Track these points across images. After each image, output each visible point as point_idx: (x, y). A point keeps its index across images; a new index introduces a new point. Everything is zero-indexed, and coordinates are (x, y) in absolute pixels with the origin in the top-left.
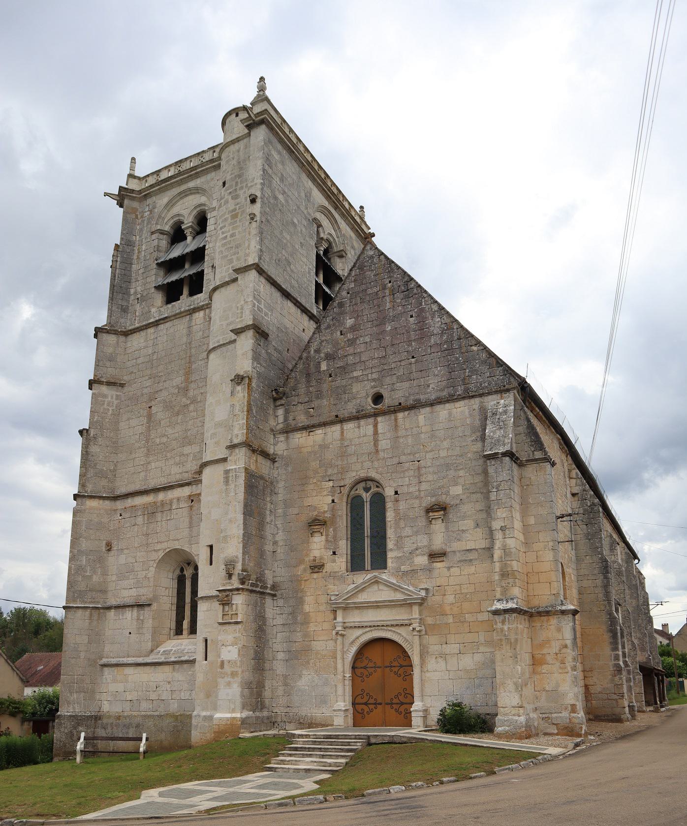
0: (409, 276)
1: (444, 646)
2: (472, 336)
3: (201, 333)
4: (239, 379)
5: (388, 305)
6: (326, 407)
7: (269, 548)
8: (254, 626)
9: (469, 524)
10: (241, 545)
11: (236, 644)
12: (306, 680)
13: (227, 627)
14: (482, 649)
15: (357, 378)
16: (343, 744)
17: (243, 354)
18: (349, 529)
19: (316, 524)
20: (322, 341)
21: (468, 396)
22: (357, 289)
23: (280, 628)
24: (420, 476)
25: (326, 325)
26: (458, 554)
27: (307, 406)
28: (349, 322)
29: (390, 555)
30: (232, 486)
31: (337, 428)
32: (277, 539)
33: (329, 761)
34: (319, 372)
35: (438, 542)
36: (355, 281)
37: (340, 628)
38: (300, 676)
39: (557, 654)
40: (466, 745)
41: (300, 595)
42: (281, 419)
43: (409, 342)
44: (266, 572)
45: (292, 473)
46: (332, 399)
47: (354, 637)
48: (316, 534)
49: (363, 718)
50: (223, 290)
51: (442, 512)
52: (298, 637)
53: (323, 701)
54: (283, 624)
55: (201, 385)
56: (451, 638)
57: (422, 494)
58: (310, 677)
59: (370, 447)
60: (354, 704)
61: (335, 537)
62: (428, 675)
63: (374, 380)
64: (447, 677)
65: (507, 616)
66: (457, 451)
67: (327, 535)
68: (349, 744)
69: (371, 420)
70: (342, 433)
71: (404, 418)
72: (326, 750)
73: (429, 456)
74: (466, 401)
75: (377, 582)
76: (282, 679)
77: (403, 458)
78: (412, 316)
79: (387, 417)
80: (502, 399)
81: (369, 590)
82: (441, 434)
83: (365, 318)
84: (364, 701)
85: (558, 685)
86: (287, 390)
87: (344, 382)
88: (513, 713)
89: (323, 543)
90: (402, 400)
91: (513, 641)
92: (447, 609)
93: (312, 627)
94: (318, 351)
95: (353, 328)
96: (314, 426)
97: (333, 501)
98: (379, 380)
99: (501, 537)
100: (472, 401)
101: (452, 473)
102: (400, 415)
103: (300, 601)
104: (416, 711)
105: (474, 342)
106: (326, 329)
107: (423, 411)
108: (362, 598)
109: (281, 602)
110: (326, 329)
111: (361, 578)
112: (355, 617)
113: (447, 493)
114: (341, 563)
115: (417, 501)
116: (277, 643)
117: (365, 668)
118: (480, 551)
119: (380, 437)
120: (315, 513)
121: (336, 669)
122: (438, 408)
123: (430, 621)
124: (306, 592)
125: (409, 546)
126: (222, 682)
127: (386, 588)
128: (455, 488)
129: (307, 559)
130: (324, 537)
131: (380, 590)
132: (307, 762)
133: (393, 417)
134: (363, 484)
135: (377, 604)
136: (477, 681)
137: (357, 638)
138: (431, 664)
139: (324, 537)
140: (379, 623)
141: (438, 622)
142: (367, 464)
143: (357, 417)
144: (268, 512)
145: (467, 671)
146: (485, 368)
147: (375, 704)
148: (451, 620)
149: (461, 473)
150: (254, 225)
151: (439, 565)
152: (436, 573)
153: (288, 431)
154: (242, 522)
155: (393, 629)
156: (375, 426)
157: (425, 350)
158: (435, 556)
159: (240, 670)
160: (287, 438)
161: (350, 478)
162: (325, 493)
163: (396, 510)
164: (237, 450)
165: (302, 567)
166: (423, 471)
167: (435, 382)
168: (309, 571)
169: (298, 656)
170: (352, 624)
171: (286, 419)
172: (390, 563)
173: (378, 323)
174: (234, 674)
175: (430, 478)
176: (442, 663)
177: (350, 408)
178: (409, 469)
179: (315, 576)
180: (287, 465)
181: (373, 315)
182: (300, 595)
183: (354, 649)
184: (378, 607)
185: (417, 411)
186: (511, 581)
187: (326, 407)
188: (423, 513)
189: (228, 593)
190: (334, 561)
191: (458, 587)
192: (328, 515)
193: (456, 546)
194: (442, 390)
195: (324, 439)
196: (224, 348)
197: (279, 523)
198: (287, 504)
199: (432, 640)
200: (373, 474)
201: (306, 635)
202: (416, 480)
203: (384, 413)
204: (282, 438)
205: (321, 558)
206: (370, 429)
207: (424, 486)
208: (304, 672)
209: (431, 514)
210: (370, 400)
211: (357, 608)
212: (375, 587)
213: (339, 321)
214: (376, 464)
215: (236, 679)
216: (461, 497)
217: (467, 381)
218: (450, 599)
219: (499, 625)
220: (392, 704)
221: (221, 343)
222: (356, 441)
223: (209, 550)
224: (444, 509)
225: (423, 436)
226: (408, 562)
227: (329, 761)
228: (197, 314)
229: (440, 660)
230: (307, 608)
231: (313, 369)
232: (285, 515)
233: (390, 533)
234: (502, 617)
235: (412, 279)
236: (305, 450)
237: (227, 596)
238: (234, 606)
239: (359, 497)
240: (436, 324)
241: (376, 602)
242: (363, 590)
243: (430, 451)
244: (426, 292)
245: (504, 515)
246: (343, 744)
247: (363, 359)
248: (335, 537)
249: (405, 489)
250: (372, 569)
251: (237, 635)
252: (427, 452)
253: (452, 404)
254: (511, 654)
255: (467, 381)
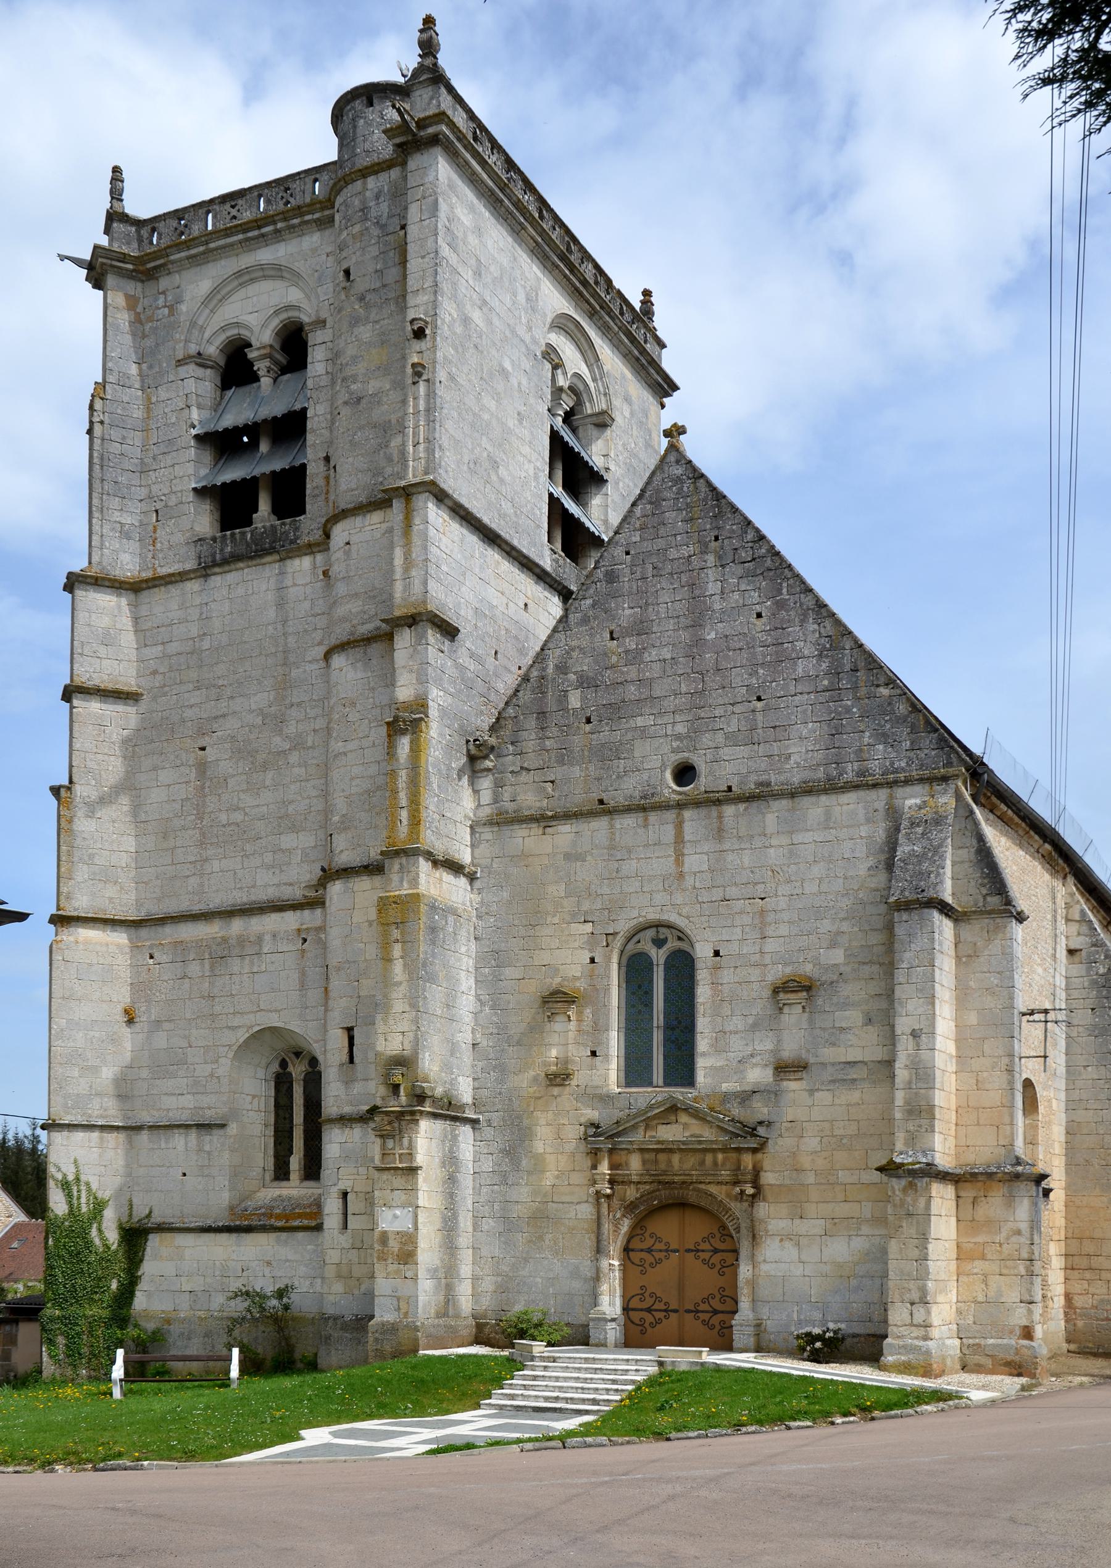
3: (307, 605)
9: (853, 1017)
14: (865, 1229)
15: (643, 729)
19: (557, 1000)
24: (764, 924)
26: (830, 1069)
27: (538, 776)
29: (701, 1063)
31: (600, 825)
46: (592, 768)
51: (805, 994)
57: (767, 959)
63: (678, 737)
69: (671, 815)
71: (736, 816)
79: (703, 812)
90: (734, 783)
94: (562, 669)
97: (592, 960)
102: (729, 810)
125: (738, 1046)
133: (714, 811)
134: (651, 933)
142: (660, 898)
148: (810, 1179)
151: (793, 1085)
156: (679, 826)
162: (577, 944)
166: (771, 917)
177: (630, 788)
185: (762, 804)
188: (767, 993)
191: (827, 1125)
192: (582, 985)
193: (828, 1054)
200: (673, 918)
206: (669, 832)
207: (771, 946)
209: (782, 995)
210: (669, 776)
214: (679, 898)
216: (842, 969)
218: (812, 1143)
226: (735, 1078)
228: (297, 562)
231: (551, 703)
233: (702, 1023)
247: (657, 693)
249: (734, 948)
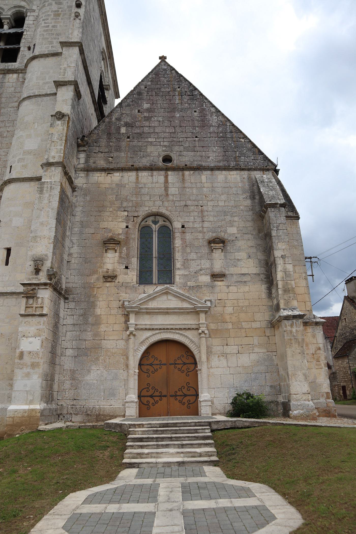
0: (194, 87)
1: (225, 347)
2: (241, 132)
3: (13, 89)
4: (60, 116)
5: (177, 101)
6: (123, 158)
7: (66, 257)
8: (53, 322)
9: (242, 255)
10: (52, 246)
11: (40, 336)
12: (94, 375)
13: (29, 319)
14: (256, 350)
15: (151, 142)
16: (189, 432)
17: (63, 101)
18: (139, 250)
19: (111, 243)
20: (123, 114)
21: (238, 168)
22: (153, 86)
23: (71, 328)
24: (203, 216)
25: (126, 104)
26: (235, 277)
27: (106, 155)
28: (146, 106)
29: (178, 273)
30: (46, 195)
31: (133, 174)
32: (71, 252)
33: (198, 450)
34: (119, 133)
35: (218, 267)
36: (151, 81)
37: (133, 329)
38: (89, 371)
39: (313, 354)
40: (333, 427)
41: (92, 299)
42: (82, 161)
43: (194, 127)
44: (63, 276)
45: (90, 201)
46: (129, 154)
47: (144, 337)
48: (109, 251)
49: (149, 409)
50: (42, 60)
51: (222, 245)
52: (89, 335)
53: (112, 394)
54: (74, 325)
55: (8, 125)
56: (231, 341)
57: (205, 230)
58: (99, 372)
59: (162, 191)
60: (139, 397)
61: (128, 255)
62: (211, 370)
63: (165, 146)
64: (228, 373)
65: (294, 321)
66: (232, 203)
67: (120, 253)
68: (196, 431)
69: (163, 173)
70: (137, 178)
71: (190, 175)
72: (163, 439)
73: (210, 203)
74: (238, 172)
75: (167, 293)
76: (69, 373)
77: (189, 203)
78: (195, 112)
79: (176, 173)
80: (264, 174)
81: (159, 299)
82: (219, 190)
83: (159, 105)
84: (150, 393)
85: (315, 378)
86: (90, 141)
87: (140, 144)
88: (304, 398)
89: (117, 259)
90: (188, 163)
91: (300, 340)
92: (227, 318)
93: (103, 328)
94: (119, 119)
95: (149, 110)
96: (113, 170)
97: (127, 227)
98: (170, 147)
99: (282, 263)
100: (243, 172)
101: (228, 218)
102: (187, 173)
103: (92, 305)
104: (205, 401)
105: (242, 136)
106: (126, 106)
107: (205, 173)
108: (153, 305)
109: (72, 305)
110: (126, 106)
111: (150, 290)
112: (146, 321)
113: (225, 232)
114: (132, 276)
115: (201, 235)
116: (68, 340)
117: (151, 365)
118: (252, 275)
119: (170, 185)
120: (110, 235)
121: (127, 366)
122: (217, 172)
123: (212, 326)
124: (98, 298)
125: (194, 266)
126: (19, 373)
127: (174, 299)
128: (231, 228)
129: (100, 270)
130: (117, 254)
131: (169, 300)
132: (172, 454)
133: (181, 173)
135: (164, 313)
136: (253, 376)
137: (147, 338)
138: (215, 361)
139: (117, 254)
140: (169, 327)
141: (220, 328)
142: (159, 203)
143: (151, 168)
144: (68, 228)
145: (244, 367)
146: (250, 154)
147: (160, 396)
148: (230, 326)
149: (236, 219)
150: (78, 21)
151: (219, 283)
152: (217, 289)
153: (88, 170)
154: (54, 226)
155: (177, 331)
156: (166, 177)
157: (206, 134)
158: (215, 276)
159: (42, 361)
160: (87, 175)
161: (143, 211)
162: (120, 220)
163: (183, 239)
164: (53, 168)
165: (95, 276)
166: (206, 213)
167: (213, 156)
168: (102, 280)
169: (87, 353)
170: (143, 327)
171: (87, 161)
172: (177, 279)
173: (169, 110)
174: (34, 365)
175: (211, 219)
176: (223, 362)
177: (145, 162)
178: (193, 211)
179: (108, 284)
180: (85, 195)
181: (165, 105)
182: (92, 299)
183: (144, 348)
184: (167, 313)
185: (200, 172)
186: (291, 295)
187: (123, 158)
188: (206, 243)
189: (34, 287)
190: (126, 274)
191: (235, 301)
192: (122, 237)
193: (232, 270)
194: (219, 162)
195: (121, 180)
196: (39, 99)
197: (75, 239)
198: (83, 225)
199: (216, 342)
200: (163, 211)
201: (96, 335)
202: (199, 220)
203: (173, 169)
204: (82, 174)
205: (114, 270)
206: (162, 179)
207: (206, 224)
208: (93, 367)
209: (212, 245)
210: (161, 159)
211: (147, 313)
212: (165, 297)
213: (137, 103)
214: (166, 204)
215: (37, 370)
216: (236, 235)
217: (237, 159)
218: (229, 310)
219: (289, 328)
220: (176, 396)
221: (36, 94)
222: (150, 185)
223: (5, 252)
224: (223, 242)
225: (205, 189)
226: (193, 280)
227: (198, 450)
228: (11, 75)
229: (222, 358)
230: (98, 311)
231: (113, 130)
232: (81, 233)
233: (178, 256)
234: (290, 322)
235: (196, 89)
236: (104, 186)
237: (33, 290)
238: (40, 300)
239: (149, 227)
240: (214, 120)
241: (167, 309)
242: (154, 298)
243: (211, 201)
244: (206, 99)
245: (284, 247)
246: (189, 432)
247: (157, 131)
248: (128, 255)
249: (191, 225)
250: (159, 284)
251: (41, 327)
252: (208, 201)
253: (228, 172)
254: (299, 351)
255: (237, 159)
